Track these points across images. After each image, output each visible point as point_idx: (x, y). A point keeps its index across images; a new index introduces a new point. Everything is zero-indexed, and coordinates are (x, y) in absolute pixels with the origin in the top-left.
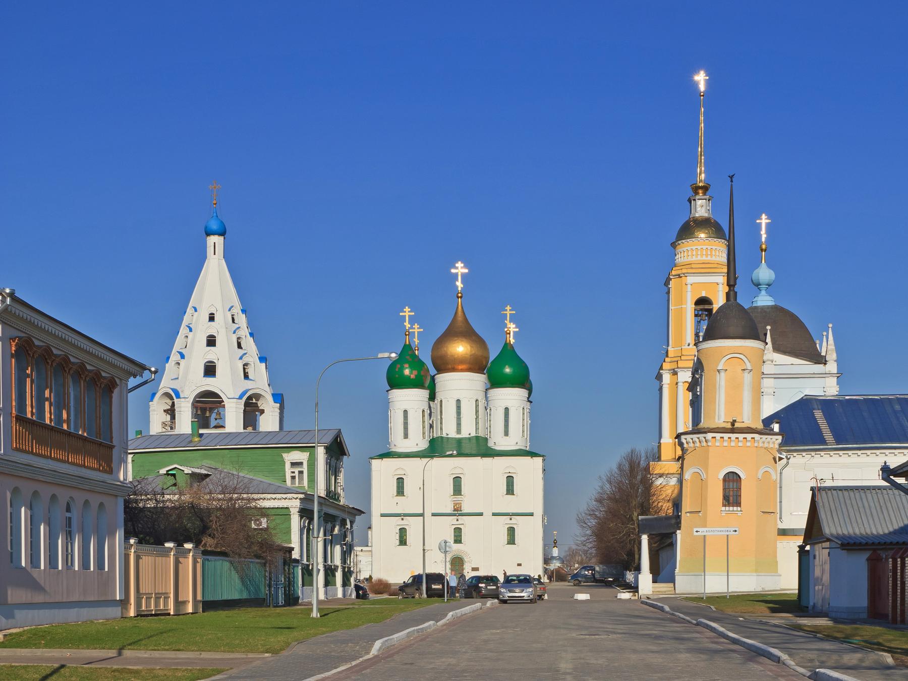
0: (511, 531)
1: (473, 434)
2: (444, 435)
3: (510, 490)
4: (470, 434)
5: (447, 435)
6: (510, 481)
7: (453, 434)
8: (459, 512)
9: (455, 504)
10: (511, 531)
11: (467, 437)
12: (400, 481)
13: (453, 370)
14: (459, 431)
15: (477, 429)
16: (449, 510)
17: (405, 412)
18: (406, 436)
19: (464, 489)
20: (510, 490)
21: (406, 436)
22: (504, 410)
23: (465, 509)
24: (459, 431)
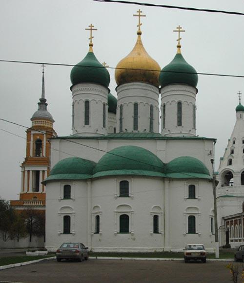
5: (126, 129)
15: (151, 128)
22: (177, 104)
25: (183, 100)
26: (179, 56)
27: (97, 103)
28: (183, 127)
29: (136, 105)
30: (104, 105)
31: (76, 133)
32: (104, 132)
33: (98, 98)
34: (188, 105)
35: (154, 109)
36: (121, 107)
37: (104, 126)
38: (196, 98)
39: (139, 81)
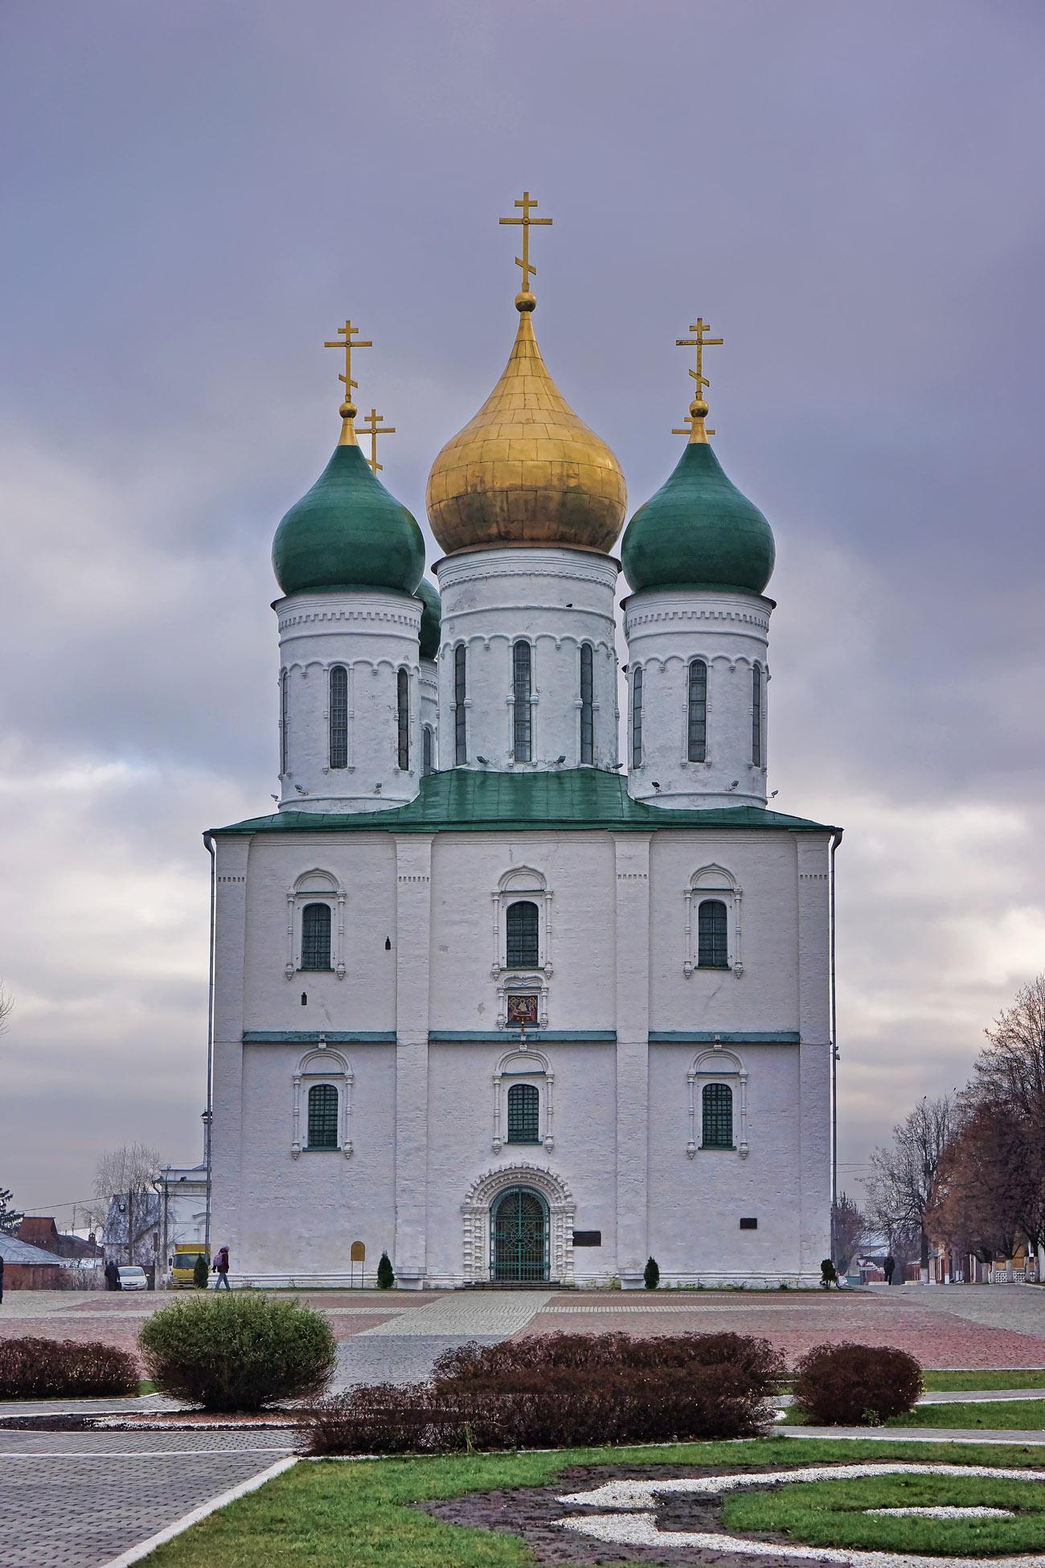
0: (717, 1101)
1: (573, 762)
2: (476, 767)
3: (713, 955)
4: (561, 760)
5: (481, 760)
6: (712, 914)
7: (502, 759)
8: (526, 1030)
9: (513, 1002)
10: (717, 1101)
11: (553, 770)
12: (317, 917)
13: (505, 540)
14: (522, 745)
16: (491, 1017)
17: (339, 674)
18: (339, 758)
19: (547, 947)
20: (713, 955)
21: (339, 758)
22: (687, 671)
23: (555, 1016)
24: (522, 745)
25: (708, 650)
26: (699, 458)
27: (375, 673)
28: (709, 765)
29: (522, 648)
30: (402, 674)
31: (296, 796)
32: (403, 791)
33: (376, 652)
34: (732, 669)
35: (598, 660)
36: (460, 650)
37: (404, 763)
38: (769, 637)
39: (535, 542)
